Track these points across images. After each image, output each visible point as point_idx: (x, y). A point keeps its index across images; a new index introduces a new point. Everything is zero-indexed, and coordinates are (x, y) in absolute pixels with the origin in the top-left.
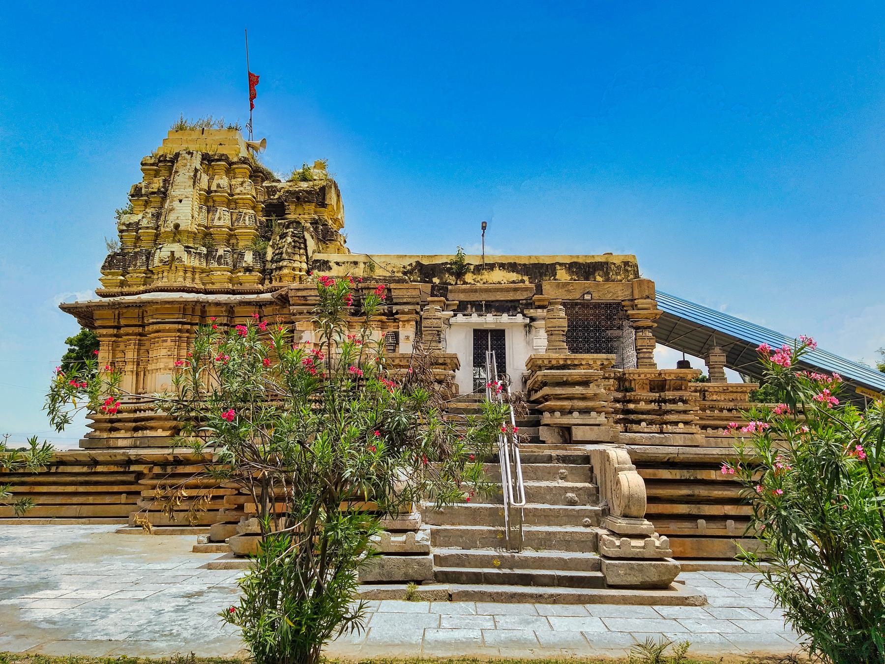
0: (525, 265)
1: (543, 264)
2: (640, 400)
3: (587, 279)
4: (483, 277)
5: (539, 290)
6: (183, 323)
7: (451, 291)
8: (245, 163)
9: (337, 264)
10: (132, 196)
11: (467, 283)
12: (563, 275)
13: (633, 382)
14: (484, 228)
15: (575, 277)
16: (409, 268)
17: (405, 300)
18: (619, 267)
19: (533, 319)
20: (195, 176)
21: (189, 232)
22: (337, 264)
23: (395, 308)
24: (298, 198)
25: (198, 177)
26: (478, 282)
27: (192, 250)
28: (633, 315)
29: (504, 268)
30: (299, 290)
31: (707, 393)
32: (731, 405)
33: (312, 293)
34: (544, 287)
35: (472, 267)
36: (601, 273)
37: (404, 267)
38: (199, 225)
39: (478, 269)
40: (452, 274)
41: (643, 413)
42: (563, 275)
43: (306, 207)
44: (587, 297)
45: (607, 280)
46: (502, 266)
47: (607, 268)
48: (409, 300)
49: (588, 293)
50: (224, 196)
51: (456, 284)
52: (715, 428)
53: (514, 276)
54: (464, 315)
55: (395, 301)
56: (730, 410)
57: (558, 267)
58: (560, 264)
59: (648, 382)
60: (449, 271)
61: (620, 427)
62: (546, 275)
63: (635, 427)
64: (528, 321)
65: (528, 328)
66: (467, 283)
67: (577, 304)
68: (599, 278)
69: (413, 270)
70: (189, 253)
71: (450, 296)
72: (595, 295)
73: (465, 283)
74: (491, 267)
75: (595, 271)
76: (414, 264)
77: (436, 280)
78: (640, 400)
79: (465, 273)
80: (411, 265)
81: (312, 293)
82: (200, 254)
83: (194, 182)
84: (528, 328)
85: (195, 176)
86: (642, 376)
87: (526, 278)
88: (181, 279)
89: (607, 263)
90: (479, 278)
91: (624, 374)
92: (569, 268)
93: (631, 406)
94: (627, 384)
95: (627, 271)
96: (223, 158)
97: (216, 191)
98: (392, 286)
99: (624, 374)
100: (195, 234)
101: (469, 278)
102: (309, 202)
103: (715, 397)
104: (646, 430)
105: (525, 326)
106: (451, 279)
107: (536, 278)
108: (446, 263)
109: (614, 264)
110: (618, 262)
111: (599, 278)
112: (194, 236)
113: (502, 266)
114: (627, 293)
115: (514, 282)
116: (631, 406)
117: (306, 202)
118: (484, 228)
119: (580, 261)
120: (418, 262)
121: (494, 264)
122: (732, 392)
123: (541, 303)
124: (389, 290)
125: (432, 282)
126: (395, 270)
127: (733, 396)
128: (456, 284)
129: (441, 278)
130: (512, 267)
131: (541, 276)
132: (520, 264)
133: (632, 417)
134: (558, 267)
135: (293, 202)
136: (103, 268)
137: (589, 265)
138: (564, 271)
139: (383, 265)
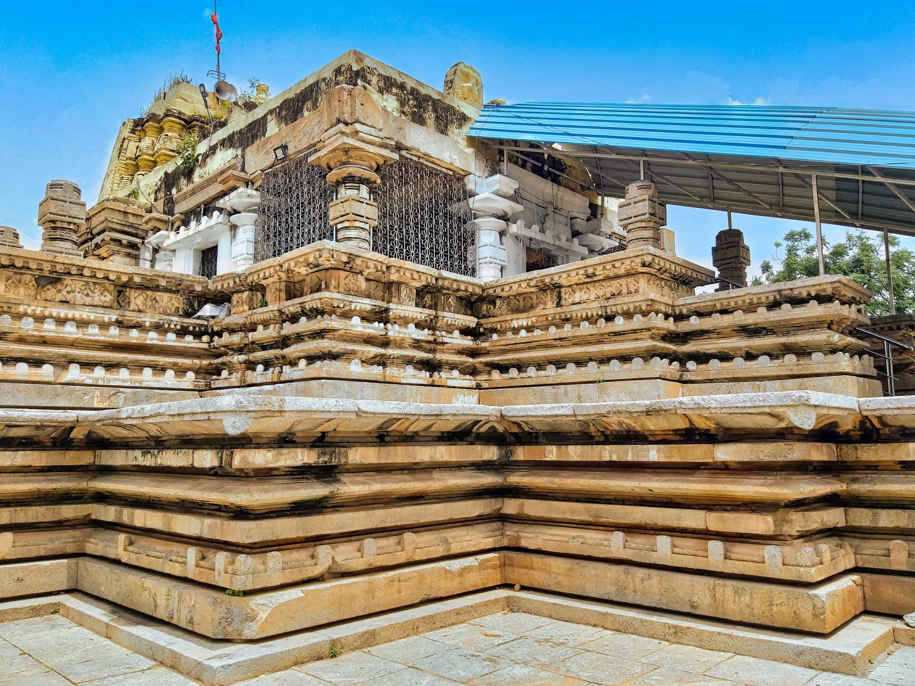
0: (240, 132)
20: (122, 146)
25: (124, 147)
31: (563, 290)
32: (594, 308)
35: (200, 158)
52: (560, 364)
56: (591, 320)
59: (283, 284)
84: (234, 228)
85: (122, 146)
89: (317, 83)
96: (153, 117)
103: (578, 296)
104: (259, 380)
110: (328, 74)
119: (292, 95)
120: (166, 173)
122: (608, 278)
127: (613, 287)
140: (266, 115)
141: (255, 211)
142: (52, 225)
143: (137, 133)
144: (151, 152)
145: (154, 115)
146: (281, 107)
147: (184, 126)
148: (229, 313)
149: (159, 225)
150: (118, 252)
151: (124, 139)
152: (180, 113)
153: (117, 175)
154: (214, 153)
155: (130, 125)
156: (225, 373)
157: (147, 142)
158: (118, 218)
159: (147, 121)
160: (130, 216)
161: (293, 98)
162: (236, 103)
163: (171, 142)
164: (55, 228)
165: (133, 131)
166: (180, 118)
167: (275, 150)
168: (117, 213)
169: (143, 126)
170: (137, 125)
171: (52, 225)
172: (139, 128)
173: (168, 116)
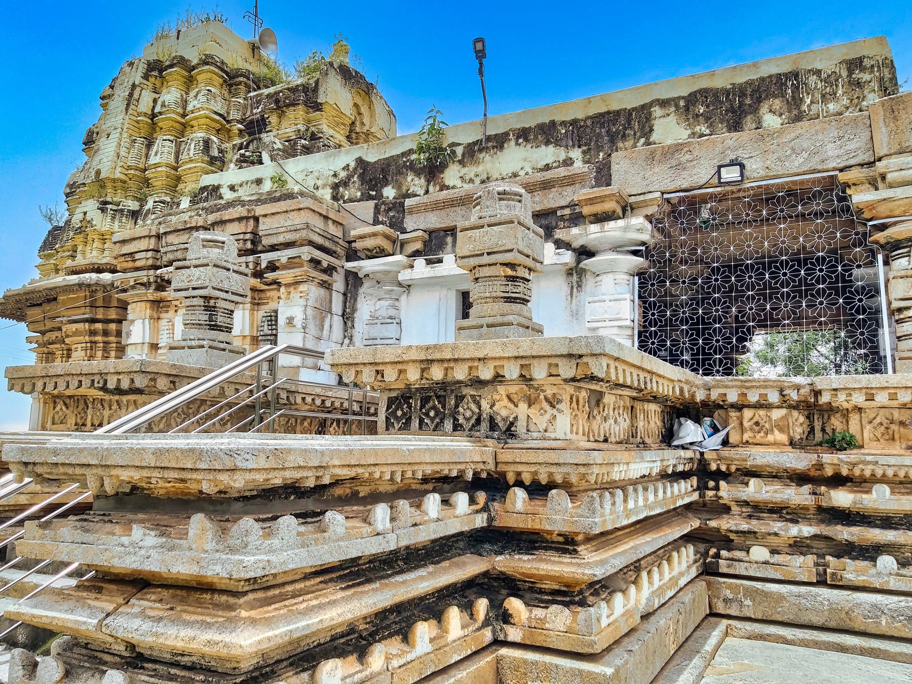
0: (574, 122)
1: (618, 113)
2: (874, 480)
3: (736, 126)
4: (480, 169)
5: (603, 176)
6: (93, 321)
7: (411, 213)
8: (207, 64)
9: (232, 188)
10: (85, 144)
11: (448, 188)
12: (669, 129)
13: (854, 419)
14: (481, 55)
15: (703, 128)
16: (343, 174)
17: (281, 239)
18: (831, 80)
19: (585, 252)
20: (131, 95)
21: (114, 181)
22: (232, 188)
23: (265, 258)
24: (277, 102)
25: (136, 96)
26: (471, 181)
27: (109, 206)
28: (872, 206)
29: (527, 140)
30: (124, 242)
33: (143, 244)
34: (614, 168)
35: (459, 151)
36: (777, 103)
37: (335, 175)
38: (130, 168)
39: (472, 151)
40: (418, 173)
41: (887, 522)
42: (669, 129)
43: (291, 113)
44: (730, 174)
45: (798, 118)
46: (524, 135)
47: (796, 88)
48: (290, 237)
49: (732, 164)
50: (170, 119)
51: (427, 192)
53: (549, 154)
54: (429, 262)
55: (266, 241)
57: (657, 111)
58: (663, 103)
60: (412, 167)
61: (802, 565)
62: (624, 137)
63: (852, 570)
64: (568, 257)
65: (576, 275)
66: (448, 188)
67: (704, 200)
68: (771, 121)
69: (349, 177)
70: (103, 210)
71: (410, 223)
72: (755, 167)
73: (444, 187)
74: (499, 142)
75: (759, 100)
76: (353, 165)
77: (389, 192)
78: (874, 480)
79: (443, 167)
80: (346, 168)
81: (143, 244)
82: (122, 211)
83: (128, 105)
84: (576, 275)
86: (882, 398)
87: (576, 154)
88: (95, 253)
89: (795, 75)
90: (470, 171)
91: (817, 393)
92: (687, 108)
93: (842, 498)
94: (836, 422)
95: (859, 84)
97: (160, 113)
98: (259, 210)
99: (817, 393)
100: (125, 182)
101: (452, 175)
102: (294, 105)
104: (894, 584)
105: (569, 273)
106: (415, 183)
107: (599, 148)
108: (411, 152)
109: (818, 72)
111: (771, 121)
112: (121, 185)
113: (524, 135)
114: (852, 146)
115: (547, 167)
116: (842, 498)
117: (288, 106)
118: (481, 55)
121: (506, 134)
123: (598, 208)
124: (256, 219)
125: (379, 196)
126: (319, 183)
128: (427, 192)
129: (399, 186)
130: (546, 133)
131: (613, 141)
132: (563, 123)
133: (844, 533)
134: (657, 111)
135: (272, 111)
136: (43, 248)
137: (741, 90)
138: (672, 119)
139: (300, 178)
140: (651, 104)
141: (635, 253)
142: (509, 272)
143: (152, 80)
144: (180, 110)
145: (182, 58)
146: (691, 100)
147: (225, 81)
148: (725, 443)
149: (387, 245)
150: (309, 280)
151: (134, 86)
152: (223, 63)
153: (125, 135)
154: (501, 147)
155: (142, 68)
156: (759, 553)
157: (171, 95)
158: (318, 223)
159: (171, 66)
160: (330, 223)
161: (727, 92)
162: (331, 64)
163: (216, 102)
164: (513, 279)
165: (146, 77)
166: (222, 70)
167: (720, 167)
168: (317, 217)
169: (161, 71)
170: (152, 70)
171: (509, 272)
172: (155, 73)
173: (206, 63)
